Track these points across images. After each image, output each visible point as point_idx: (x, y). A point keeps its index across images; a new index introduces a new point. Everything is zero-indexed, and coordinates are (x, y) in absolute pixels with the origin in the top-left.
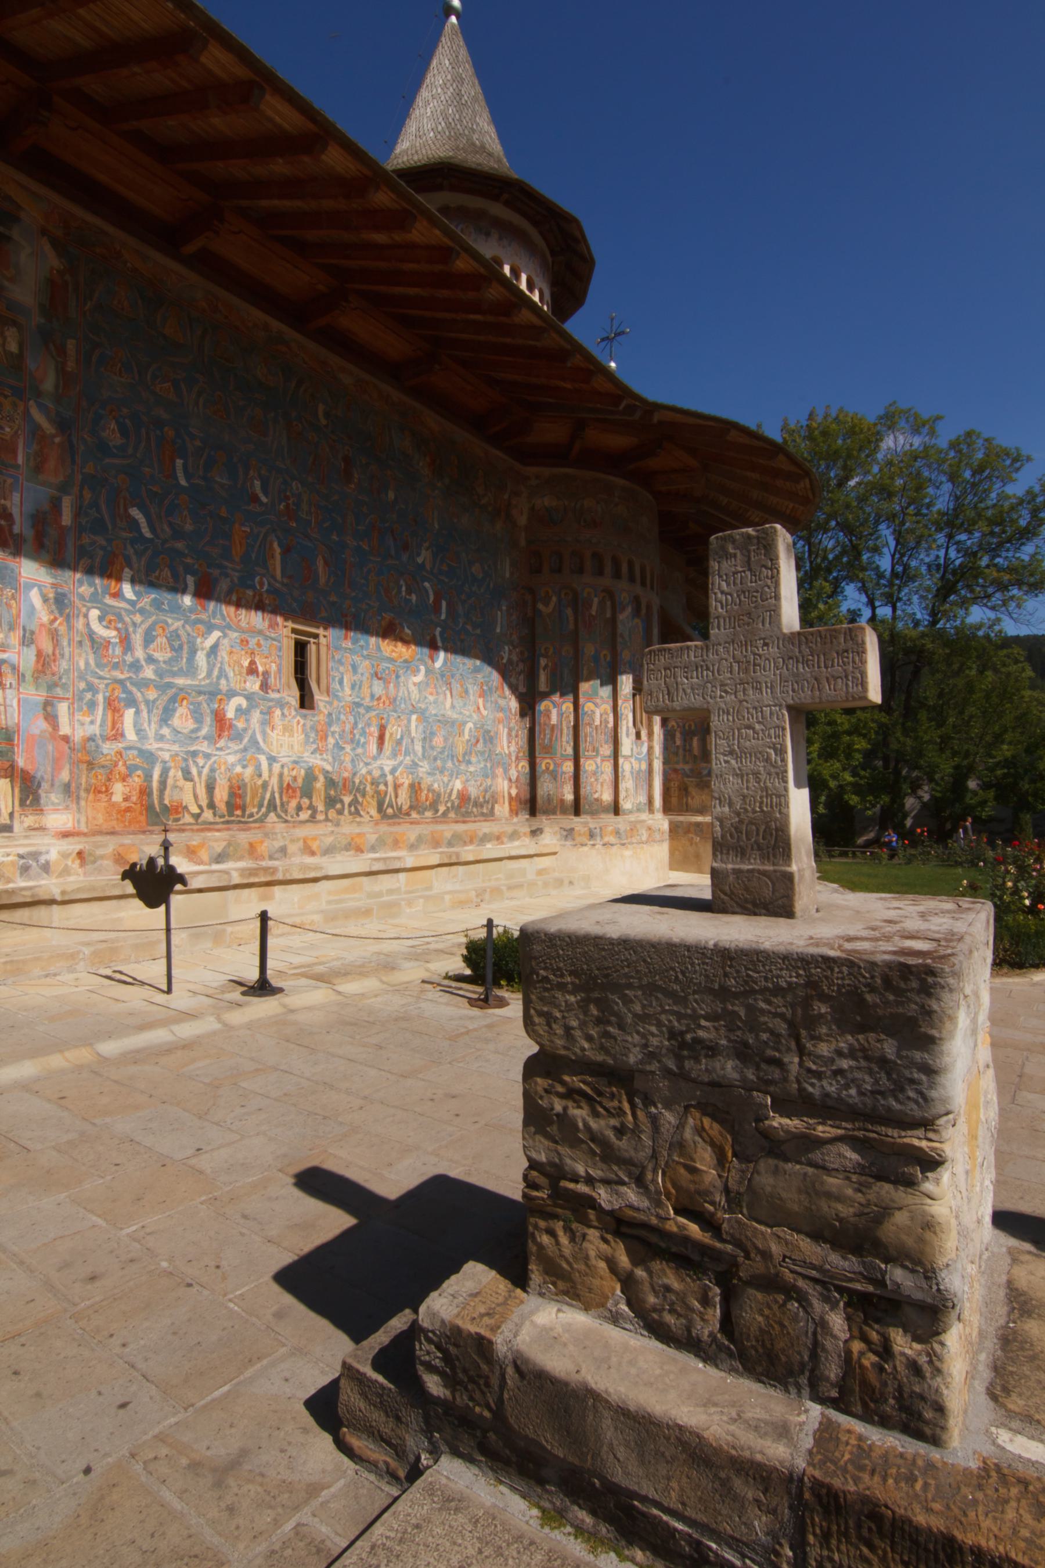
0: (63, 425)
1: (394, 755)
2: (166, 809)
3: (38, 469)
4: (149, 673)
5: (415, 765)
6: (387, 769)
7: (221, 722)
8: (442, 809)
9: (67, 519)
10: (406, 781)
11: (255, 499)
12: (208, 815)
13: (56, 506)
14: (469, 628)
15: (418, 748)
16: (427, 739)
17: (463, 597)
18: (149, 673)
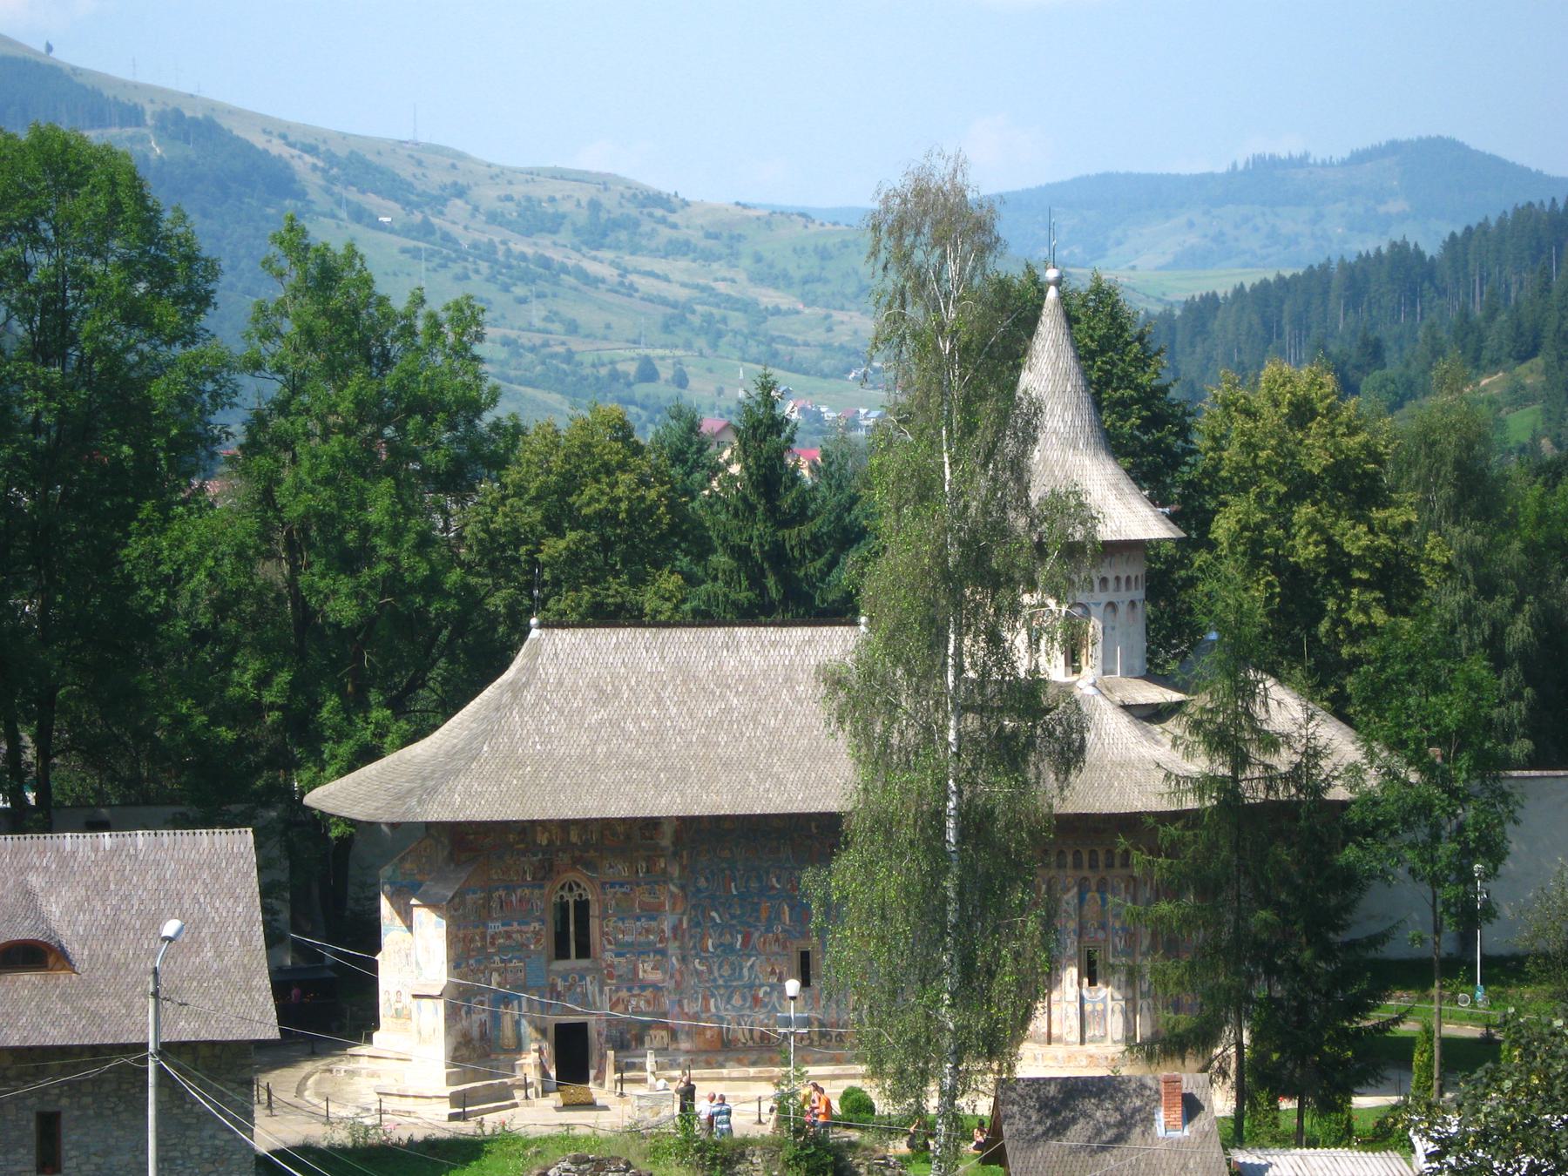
0: (683, 888)
2: (730, 1041)
3: (673, 909)
4: (721, 982)
7: (756, 1000)
9: (685, 925)
11: (773, 887)
12: (750, 1043)
13: (681, 921)
18: (721, 982)
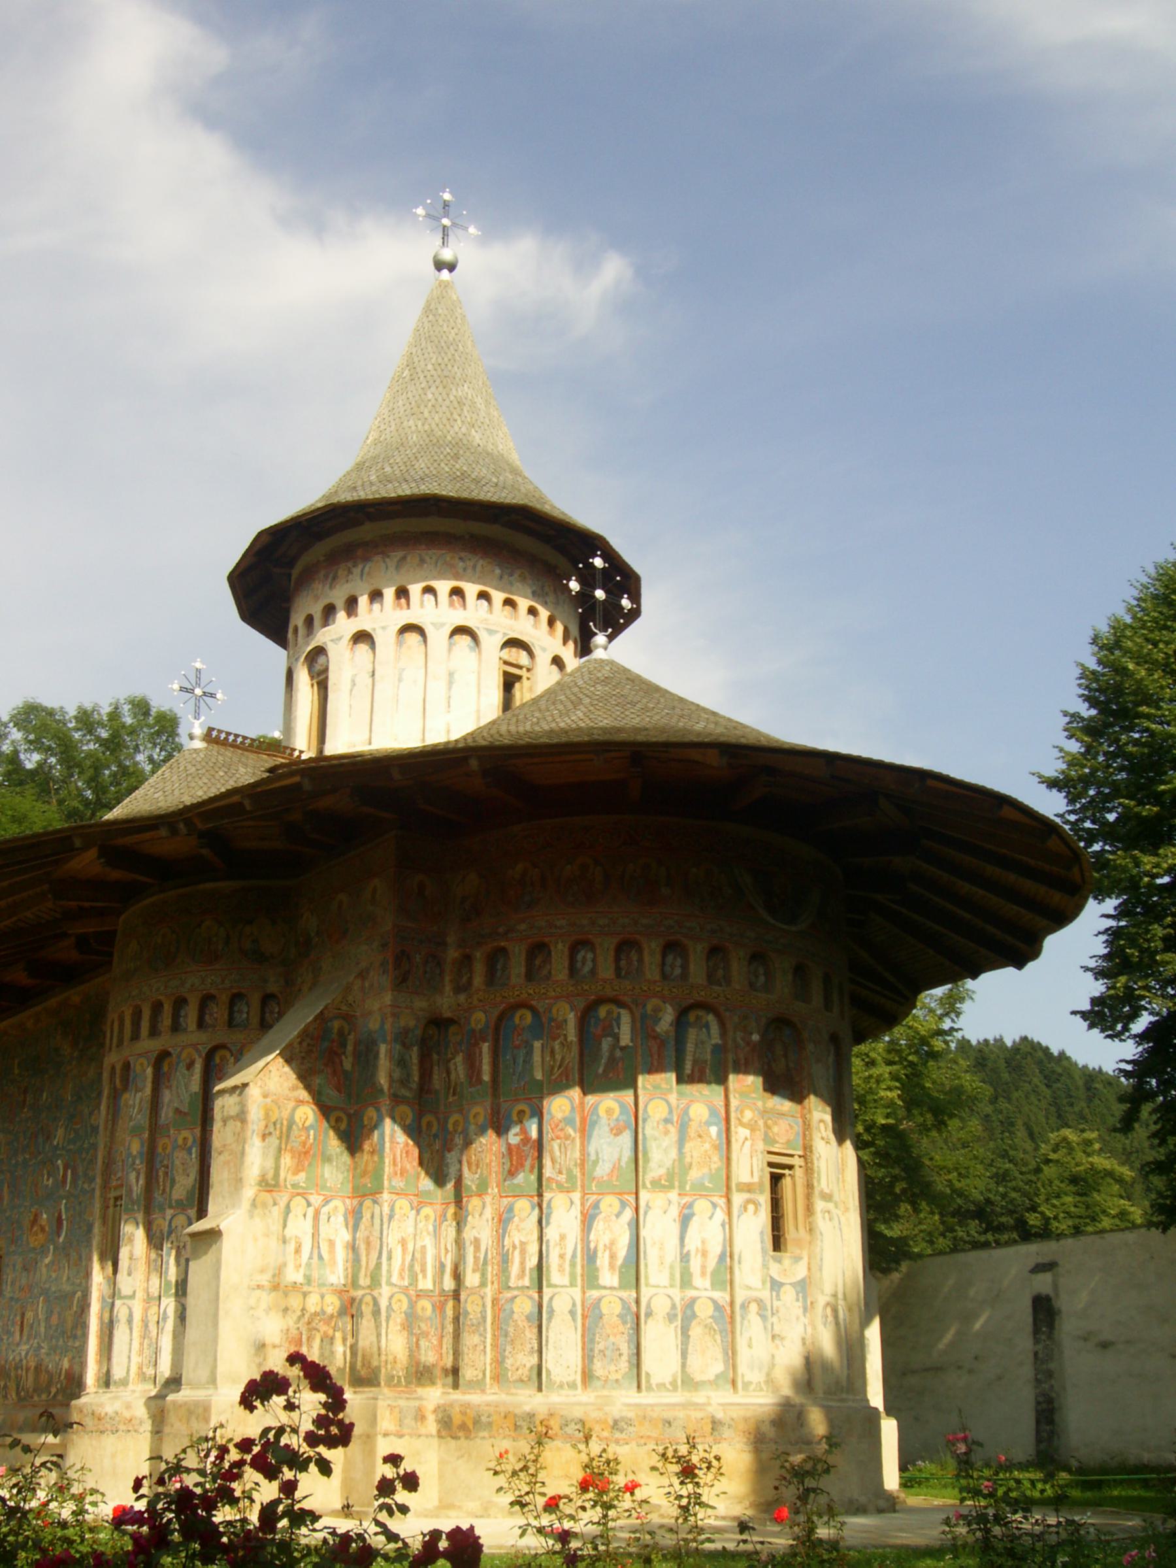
1: (28, 1339)
5: (40, 1347)
6: (23, 1353)
8: (53, 1390)
10: (32, 1364)
14: (86, 1186)
15: (42, 1329)
16: (48, 1319)
17: (84, 1155)
